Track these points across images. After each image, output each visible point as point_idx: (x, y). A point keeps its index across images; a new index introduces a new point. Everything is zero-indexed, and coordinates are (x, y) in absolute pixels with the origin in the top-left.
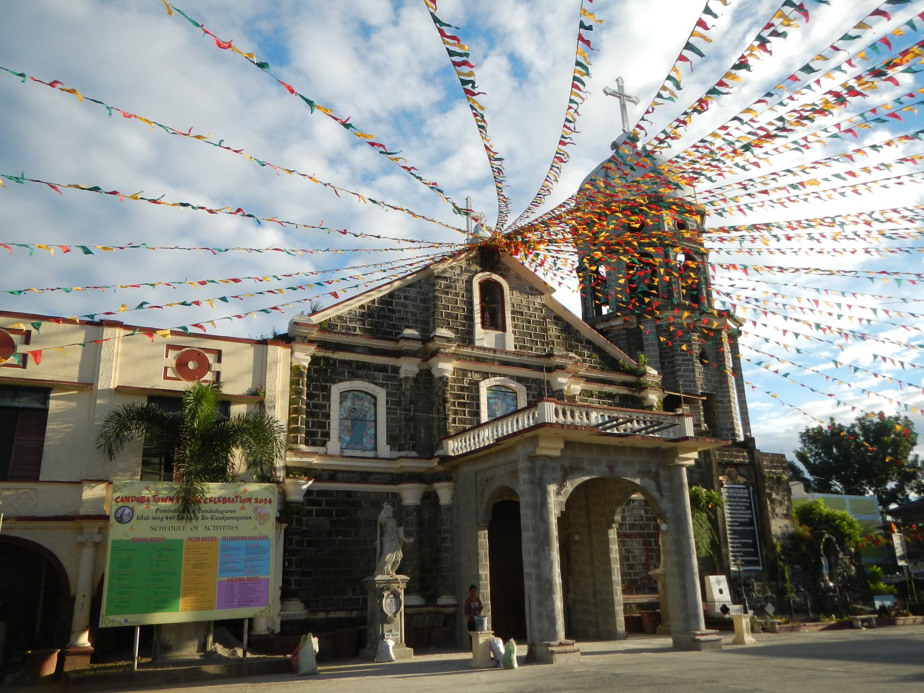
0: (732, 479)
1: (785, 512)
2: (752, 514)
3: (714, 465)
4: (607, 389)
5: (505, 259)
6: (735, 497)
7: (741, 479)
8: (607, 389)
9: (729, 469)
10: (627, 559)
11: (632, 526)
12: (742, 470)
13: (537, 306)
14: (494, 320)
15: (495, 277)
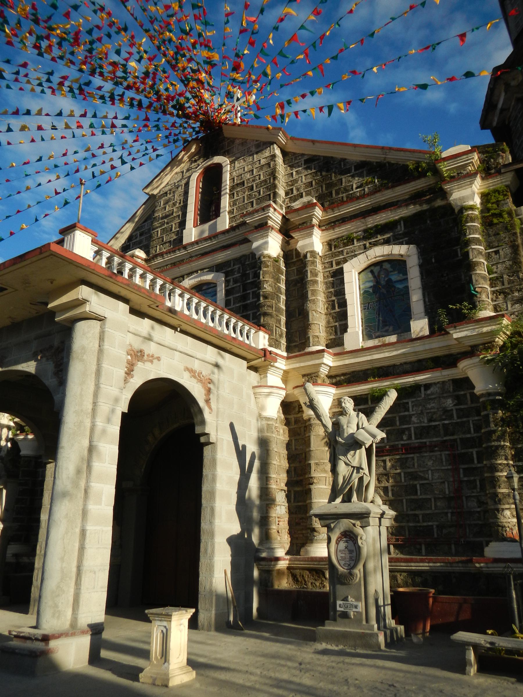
4: (372, 221)
5: (227, 132)
8: (372, 221)
10: (413, 490)
11: (422, 432)
13: (263, 162)
14: (209, 210)
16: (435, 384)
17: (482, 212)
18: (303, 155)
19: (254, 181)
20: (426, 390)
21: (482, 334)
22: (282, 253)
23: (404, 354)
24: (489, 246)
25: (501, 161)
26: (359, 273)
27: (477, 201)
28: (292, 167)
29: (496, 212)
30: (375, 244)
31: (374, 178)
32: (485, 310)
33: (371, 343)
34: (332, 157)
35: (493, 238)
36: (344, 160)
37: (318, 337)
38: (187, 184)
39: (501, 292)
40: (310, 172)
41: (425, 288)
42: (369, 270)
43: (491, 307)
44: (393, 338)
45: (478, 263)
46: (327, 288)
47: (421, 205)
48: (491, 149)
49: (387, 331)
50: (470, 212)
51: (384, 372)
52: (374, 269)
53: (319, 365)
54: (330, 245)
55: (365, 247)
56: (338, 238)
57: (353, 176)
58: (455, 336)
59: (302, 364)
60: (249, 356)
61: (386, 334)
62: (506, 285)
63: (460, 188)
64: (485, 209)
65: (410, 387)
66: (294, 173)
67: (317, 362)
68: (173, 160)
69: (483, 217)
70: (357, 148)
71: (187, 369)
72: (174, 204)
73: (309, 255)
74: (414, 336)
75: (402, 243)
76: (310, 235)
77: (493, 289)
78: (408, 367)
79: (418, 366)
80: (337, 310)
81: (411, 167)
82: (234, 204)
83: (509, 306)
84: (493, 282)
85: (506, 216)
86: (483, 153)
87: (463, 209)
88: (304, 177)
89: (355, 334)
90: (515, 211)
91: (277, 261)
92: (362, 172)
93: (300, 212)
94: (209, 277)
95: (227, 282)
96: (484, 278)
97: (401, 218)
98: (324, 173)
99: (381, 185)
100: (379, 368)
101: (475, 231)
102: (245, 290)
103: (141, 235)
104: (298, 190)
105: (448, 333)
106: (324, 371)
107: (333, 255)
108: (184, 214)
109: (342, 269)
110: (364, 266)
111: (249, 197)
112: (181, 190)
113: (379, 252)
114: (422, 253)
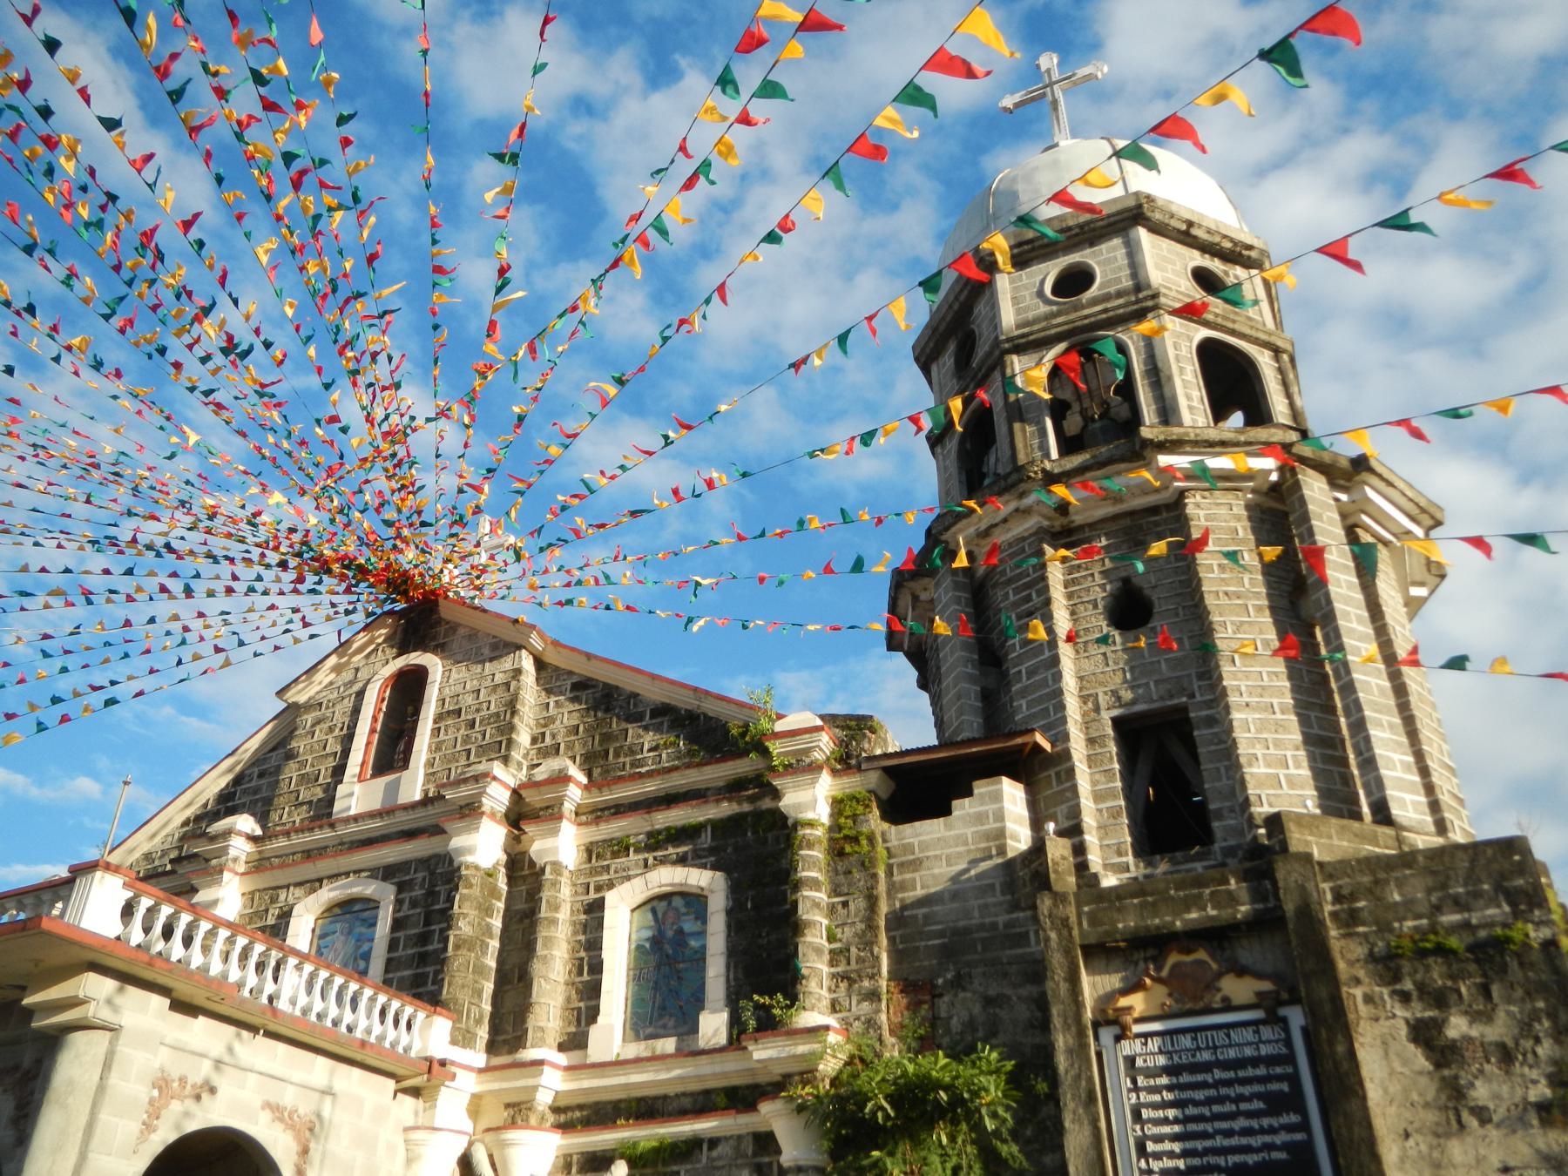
0: (1190, 994)
1: (1541, 1091)
2: (1305, 1126)
3: (1057, 960)
6: (1206, 1067)
7: (1239, 989)
9: (1173, 958)
12: (1248, 953)
13: (499, 678)
14: (392, 752)
15: (416, 658)
16: (727, 1139)
17: (831, 829)
18: (570, 673)
19: (478, 710)
20: (710, 1148)
21: (794, 1056)
22: (505, 857)
23: (680, 1078)
24: (835, 892)
25: (866, 746)
26: (633, 911)
27: (822, 813)
28: (549, 692)
29: (851, 833)
30: (662, 861)
31: (678, 737)
32: (812, 1009)
33: (635, 1050)
34: (617, 687)
35: (841, 878)
36: (635, 695)
37: (542, 1029)
38: (360, 694)
39: (844, 977)
40: (577, 707)
41: (732, 953)
42: (648, 907)
43: (826, 1003)
44: (668, 1045)
45: (809, 924)
46: (575, 933)
47: (739, 803)
48: (853, 723)
49: (664, 1027)
50: (808, 831)
51: (646, 1108)
52: (660, 905)
53: (535, 1088)
54: (590, 851)
55: (646, 866)
56: (604, 841)
57: (646, 728)
58: (757, 1055)
59: (505, 1085)
60: (400, 1071)
61: (662, 1031)
62: (854, 965)
63: (797, 787)
64: (835, 827)
65: (685, 1142)
66: (552, 705)
67: (530, 1082)
68: (341, 645)
69: (831, 839)
70: (657, 683)
71: (268, 1105)
72: (331, 730)
73: (548, 869)
74: (702, 1044)
75: (704, 866)
76: (555, 832)
77: (833, 970)
78: (687, 1102)
79: (702, 1103)
80: (586, 977)
81: (734, 732)
82: (438, 749)
83: (854, 1002)
84: (835, 957)
85: (864, 842)
86: (842, 728)
87: (797, 824)
88: (567, 715)
89: (611, 1031)
90: (883, 834)
91: (490, 875)
92: (661, 724)
93: (543, 789)
94: (369, 889)
95: (399, 903)
96: (818, 951)
97: (709, 820)
98: (600, 714)
99: (690, 753)
100: (640, 1100)
101: (813, 864)
102: (427, 923)
103: (261, 775)
104: (553, 736)
105: (745, 1048)
106: (544, 1099)
107: (593, 872)
108: (346, 753)
109: (603, 899)
110: (641, 897)
111: (466, 740)
112: (348, 704)
113: (668, 877)
114: (735, 889)
